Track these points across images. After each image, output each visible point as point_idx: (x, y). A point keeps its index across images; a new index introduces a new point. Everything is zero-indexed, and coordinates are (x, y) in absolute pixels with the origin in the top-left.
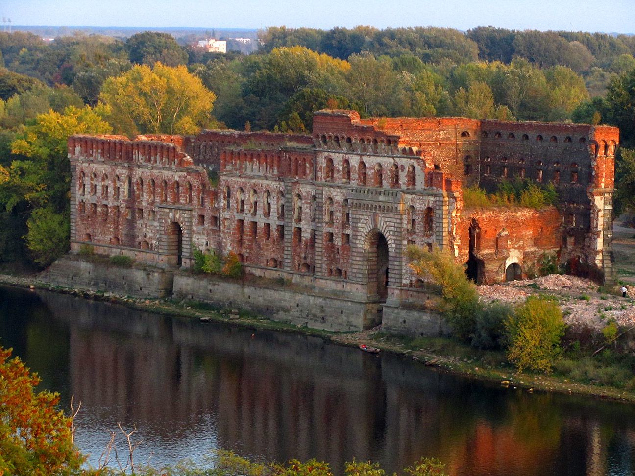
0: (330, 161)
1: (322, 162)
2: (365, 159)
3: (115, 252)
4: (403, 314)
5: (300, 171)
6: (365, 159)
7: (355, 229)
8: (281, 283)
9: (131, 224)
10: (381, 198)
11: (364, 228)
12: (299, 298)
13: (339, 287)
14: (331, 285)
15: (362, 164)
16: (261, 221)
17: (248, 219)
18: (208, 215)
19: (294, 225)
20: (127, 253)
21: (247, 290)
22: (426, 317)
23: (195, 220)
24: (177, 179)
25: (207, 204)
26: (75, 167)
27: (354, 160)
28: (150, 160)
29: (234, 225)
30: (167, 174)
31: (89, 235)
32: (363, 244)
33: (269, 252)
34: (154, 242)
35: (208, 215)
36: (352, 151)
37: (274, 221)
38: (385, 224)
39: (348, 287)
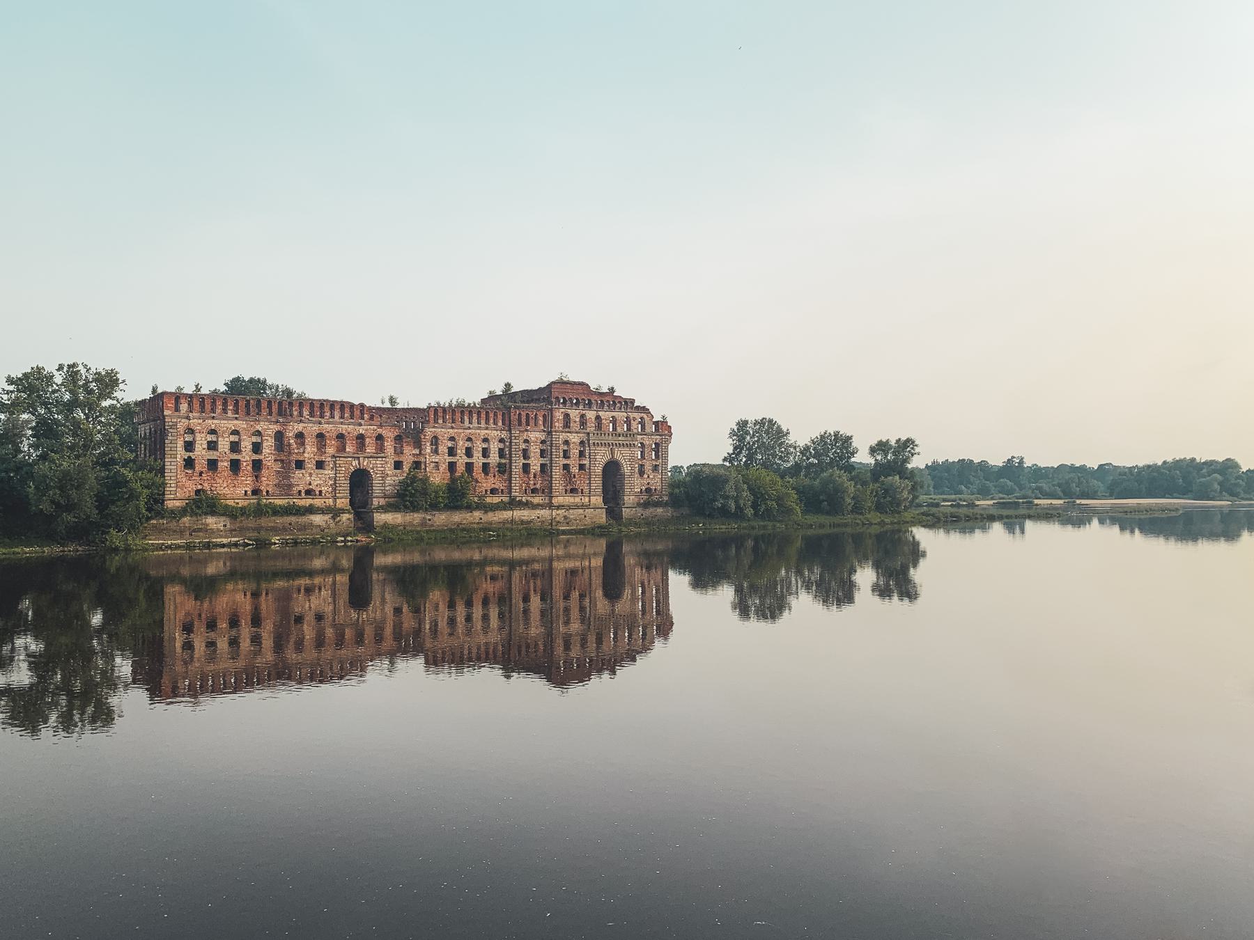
0: (567, 416)
1: (559, 415)
5: (532, 422)
8: (513, 504)
13: (577, 500)
14: (569, 500)
15: (598, 418)
17: (461, 460)
21: (477, 514)
22: (660, 510)
26: (174, 426)
27: (590, 415)
28: (322, 417)
29: (444, 467)
30: (343, 429)
33: (487, 483)
34: (324, 489)
37: (494, 459)
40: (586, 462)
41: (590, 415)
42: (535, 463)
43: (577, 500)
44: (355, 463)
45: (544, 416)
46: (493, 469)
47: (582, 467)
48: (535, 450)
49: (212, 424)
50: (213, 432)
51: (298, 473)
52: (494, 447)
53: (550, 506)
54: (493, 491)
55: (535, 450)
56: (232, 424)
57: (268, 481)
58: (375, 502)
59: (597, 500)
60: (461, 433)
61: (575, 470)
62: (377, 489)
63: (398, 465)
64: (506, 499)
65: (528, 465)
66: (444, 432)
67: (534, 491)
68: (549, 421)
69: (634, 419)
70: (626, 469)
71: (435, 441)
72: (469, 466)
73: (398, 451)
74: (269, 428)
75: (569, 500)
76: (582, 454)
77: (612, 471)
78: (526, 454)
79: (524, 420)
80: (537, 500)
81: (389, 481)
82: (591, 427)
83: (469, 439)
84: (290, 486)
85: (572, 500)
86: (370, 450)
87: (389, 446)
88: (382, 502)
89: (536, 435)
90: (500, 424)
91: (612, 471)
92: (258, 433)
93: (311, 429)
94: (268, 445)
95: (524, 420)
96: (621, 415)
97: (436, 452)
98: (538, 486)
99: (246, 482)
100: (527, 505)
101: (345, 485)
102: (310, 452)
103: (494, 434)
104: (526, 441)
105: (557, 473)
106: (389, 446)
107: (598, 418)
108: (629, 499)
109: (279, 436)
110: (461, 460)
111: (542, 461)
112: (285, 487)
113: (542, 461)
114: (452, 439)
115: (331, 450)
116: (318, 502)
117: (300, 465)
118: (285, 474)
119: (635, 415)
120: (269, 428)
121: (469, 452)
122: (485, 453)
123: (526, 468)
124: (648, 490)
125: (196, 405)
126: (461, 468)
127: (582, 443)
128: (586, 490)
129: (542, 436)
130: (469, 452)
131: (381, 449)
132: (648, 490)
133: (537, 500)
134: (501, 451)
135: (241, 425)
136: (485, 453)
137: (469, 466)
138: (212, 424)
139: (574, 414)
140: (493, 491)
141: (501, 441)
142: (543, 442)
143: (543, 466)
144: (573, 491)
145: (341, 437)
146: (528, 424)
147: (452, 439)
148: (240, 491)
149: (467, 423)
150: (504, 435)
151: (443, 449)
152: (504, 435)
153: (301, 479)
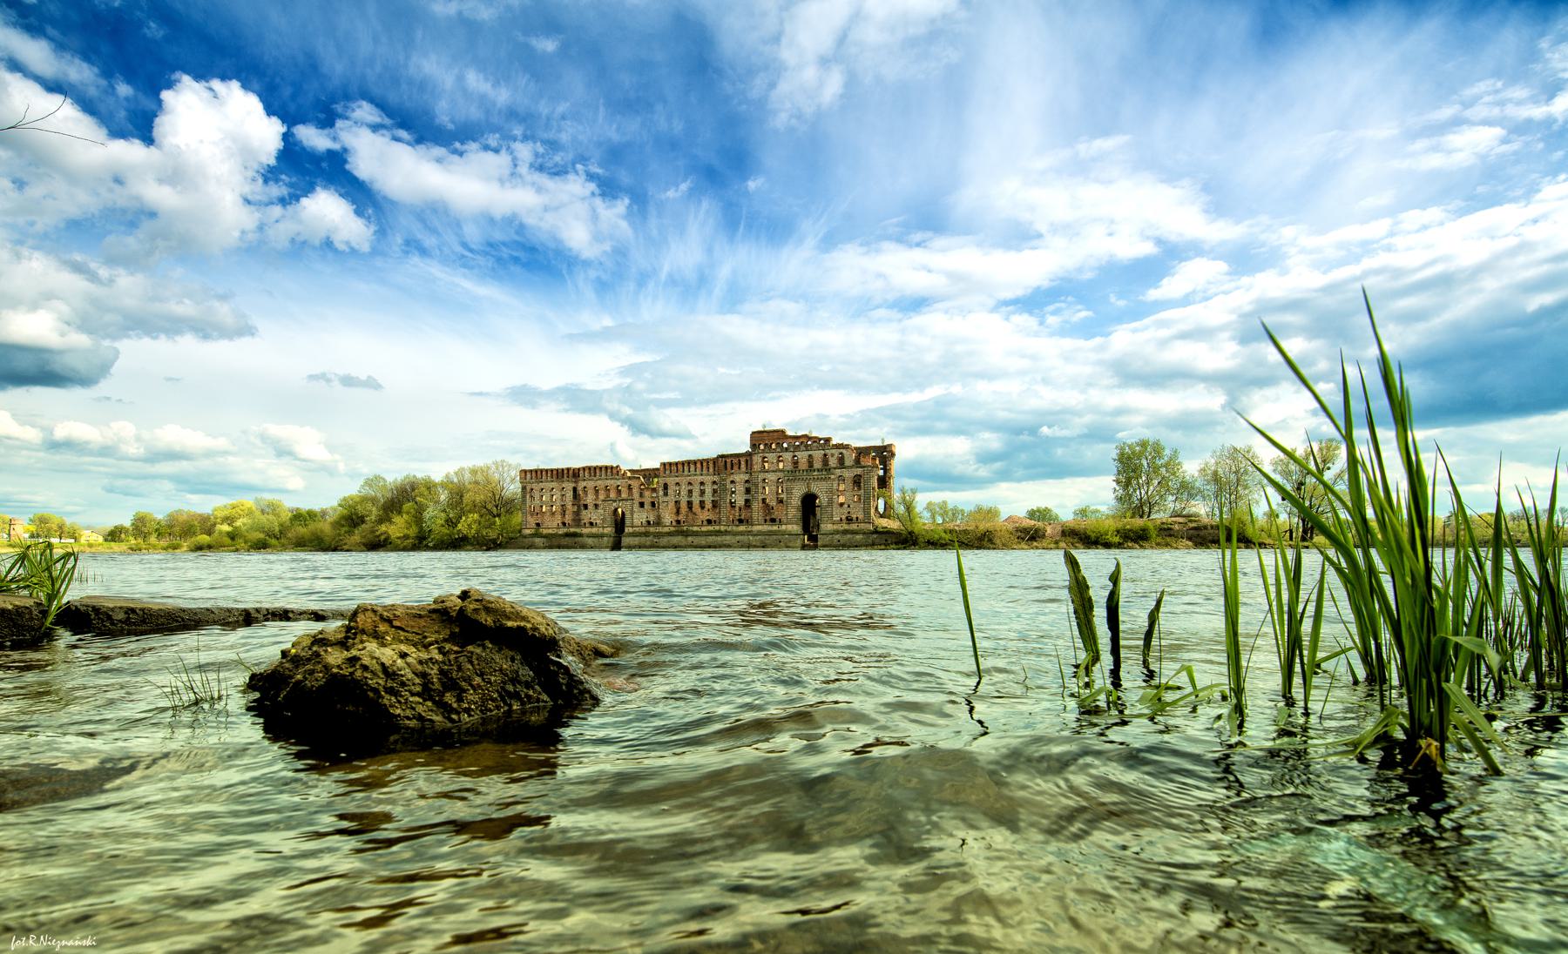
7: (789, 492)
9: (577, 513)
11: (799, 491)
14: (766, 528)
16: (696, 499)
18: (647, 501)
23: (636, 506)
25: (647, 493)
29: (672, 505)
32: (796, 501)
33: (705, 515)
35: (647, 501)
37: (708, 498)
38: (816, 488)
40: (784, 496)
42: (740, 500)
46: (709, 505)
52: (708, 489)
54: (709, 522)
55: (740, 488)
56: (552, 485)
57: (568, 518)
59: (796, 528)
60: (684, 481)
61: (773, 503)
63: (642, 505)
66: (671, 481)
67: (741, 521)
68: (749, 464)
70: (822, 499)
71: (666, 487)
72: (690, 504)
73: (641, 495)
74: (569, 486)
75: (766, 528)
77: (809, 502)
80: (742, 528)
86: (624, 495)
87: (636, 492)
89: (740, 477)
91: (809, 502)
93: (590, 484)
94: (570, 494)
97: (666, 494)
99: (558, 519)
101: (609, 519)
103: (708, 479)
105: (756, 506)
106: (636, 492)
109: (575, 489)
112: (577, 521)
115: (602, 497)
116: (594, 530)
117: (586, 507)
118: (577, 513)
122: (702, 493)
126: (684, 505)
129: (746, 477)
132: (849, 520)
134: (715, 491)
136: (702, 493)
137: (690, 504)
138: (542, 485)
140: (709, 522)
143: (747, 501)
144: (773, 520)
150: (716, 478)
152: (716, 478)
153: (586, 516)
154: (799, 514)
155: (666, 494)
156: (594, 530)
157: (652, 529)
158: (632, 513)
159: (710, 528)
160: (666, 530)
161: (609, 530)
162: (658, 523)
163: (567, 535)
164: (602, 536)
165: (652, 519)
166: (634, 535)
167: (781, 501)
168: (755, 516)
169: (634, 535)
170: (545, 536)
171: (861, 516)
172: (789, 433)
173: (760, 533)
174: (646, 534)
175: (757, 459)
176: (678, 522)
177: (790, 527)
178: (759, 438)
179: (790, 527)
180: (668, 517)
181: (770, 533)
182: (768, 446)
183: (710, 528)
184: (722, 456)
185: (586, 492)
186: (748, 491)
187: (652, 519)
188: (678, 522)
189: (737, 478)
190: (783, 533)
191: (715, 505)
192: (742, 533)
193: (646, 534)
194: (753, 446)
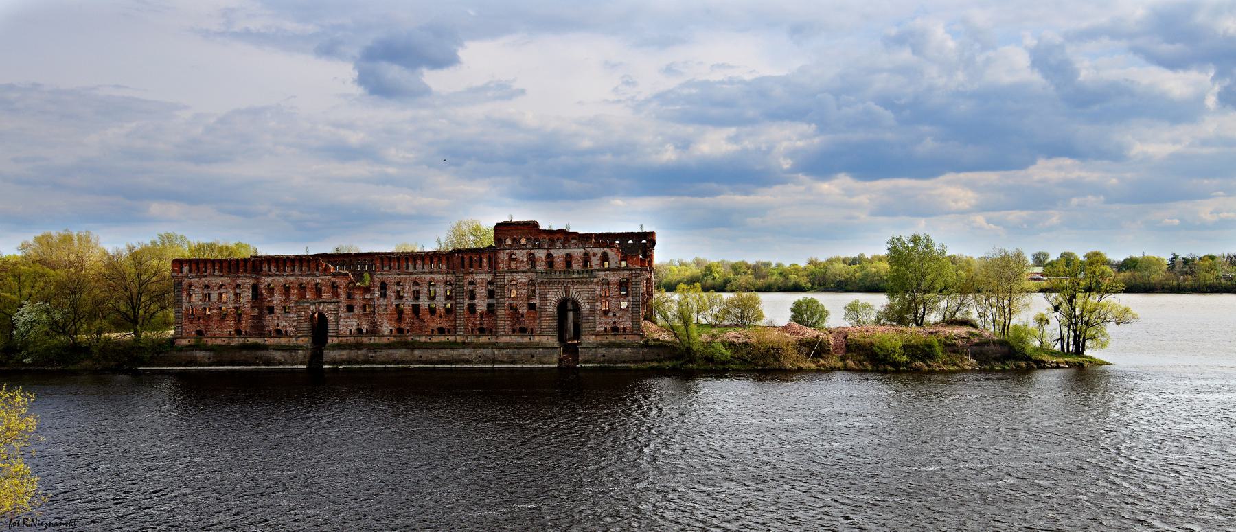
2: (552, 251)
3: (236, 342)
4: (602, 351)
5: (476, 264)
6: (552, 251)
7: (544, 298)
8: (453, 346)
9: (259, 319)
10: (575, 276)
11: (554, 296)
12: (479, 352)
13: (526, 340)
14: (515, 339)
15: (549, 256)
16: (424, 302)
19: (467, 302)
20: (259, 341)
23: (343, 309)
24: (318, 281)
25: (358, 295)
27: (541, 254)
30: (304, 279)
31: (199, 333)
32: (552, 309)
33: (436, 323)
36: (540, 247)
37: (440, 302)
38: (578, 294)
39: (537, 339)
40: (536, 301)
41: (541, 254)
42: (481, 305)
43: (526, 340)
44: (313, 308)
45: (490, 259)
47: (532, 307)
48: (481, 291)
49: (206, 281)
50: (207, 286)
51: (269, 317)
52: (440, 291)
53: (493, 345)
54: (441, 331)
55: (481, 291)
56: (219, 281)
57: (246, 325)
58: (329, 341)
59: (552, 340)
61: (523, 310)
62: (331, 330)
63: (350, 308)
64: (452, 339)
65: (474, 305)
66: (391, 278)
67: (482, 331)
68: (493, 267)
69: (595, 255)
70: (585, 307)
71: (383, 287)
72: (416, 309)
74: (249, 282)
75: (515, 339)
76: (531, 295)
78: (473, 297)
79: (467, 262)
80: (483, 339)
81: (342, 322)
82: (541, 266)
83: (415, 283)
84: (263, 327)
85: (520, 340)
87: (342, 294)
88: (336, 341)
89: (482, 277)
90: (444, 267)
92: (238, 286)
94: (247, 295)
95: (467, 262)
96: (577, 253)
97: (383, 295)
98: (485, 326)
100: (464, 345)
101: (305, 327)
102: (277, 300)
104: (471, 283)
105: (502, 313)
106: (342, 294)
107: (549, 256)
108: (588, 339)
109: (255, 288)
110: (408, 303)
111: (491, 301)
112: (259, 329)
113: (491, 301)
114: (398, 283)
115: (293, 298)
116: (283, 341)
117: (271, 310)
118: (259, 319)
119: (596, 250)
120: (249, 282)
121: (416, 296)
123: (472, 309)
124: (615, 330)
125: (194, 266)
127: (531, 283)
128: (537, 328)
129: (489, 277)
130: (416, 296)
131: (335, 293)
132: (615, 330)
133: (483, 339)
135: (226, 280)
137: (416, 309)
138: (206, 281)
139: (521, 254)
141: (446, 283)
142: (490, 283)
144: (523, 331)
145: (302, 288)
146: (471, 267)
147: (398, 283)
148: (226, 332)
149: (411, 269)
151: (389, 293)
152: (450, 277)
154: (555, 324)
155: (383, 295)
156: (283, 341)
157: (365, 340)
158: (338, 318)
159: (443, 339)
160: (384, 340)
161: (305, 340)
162: (374, 331)
163: (245, 347)
164: (296, 348)
165: (364, 326)
166: (340, 347)
167: (532, 307)
168: (501, 324)
169: (340, 347)
170: (211, 349)
171: (628, 325)
172: (544, 226)
173: (507, 346)
174: (358, 346)
175: (503, 256)
176: (400, 330)
177: (544, 339)
178: (501, 229)
179: (544, 339)
180: (386, 327)
181: (521, 346)
182: (516, 241)
183: (443, 339)
184: (459, 251)
185: (271, 290)
186: (491, 294)
187: (364, 326)
188: (400, 330)
189: (478, 278)
190: (537, 346)
191: (448, 311)
192: (483, 346)
193: (358, 346)
194: (498, 239)
